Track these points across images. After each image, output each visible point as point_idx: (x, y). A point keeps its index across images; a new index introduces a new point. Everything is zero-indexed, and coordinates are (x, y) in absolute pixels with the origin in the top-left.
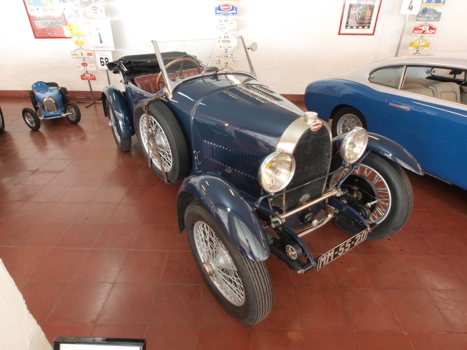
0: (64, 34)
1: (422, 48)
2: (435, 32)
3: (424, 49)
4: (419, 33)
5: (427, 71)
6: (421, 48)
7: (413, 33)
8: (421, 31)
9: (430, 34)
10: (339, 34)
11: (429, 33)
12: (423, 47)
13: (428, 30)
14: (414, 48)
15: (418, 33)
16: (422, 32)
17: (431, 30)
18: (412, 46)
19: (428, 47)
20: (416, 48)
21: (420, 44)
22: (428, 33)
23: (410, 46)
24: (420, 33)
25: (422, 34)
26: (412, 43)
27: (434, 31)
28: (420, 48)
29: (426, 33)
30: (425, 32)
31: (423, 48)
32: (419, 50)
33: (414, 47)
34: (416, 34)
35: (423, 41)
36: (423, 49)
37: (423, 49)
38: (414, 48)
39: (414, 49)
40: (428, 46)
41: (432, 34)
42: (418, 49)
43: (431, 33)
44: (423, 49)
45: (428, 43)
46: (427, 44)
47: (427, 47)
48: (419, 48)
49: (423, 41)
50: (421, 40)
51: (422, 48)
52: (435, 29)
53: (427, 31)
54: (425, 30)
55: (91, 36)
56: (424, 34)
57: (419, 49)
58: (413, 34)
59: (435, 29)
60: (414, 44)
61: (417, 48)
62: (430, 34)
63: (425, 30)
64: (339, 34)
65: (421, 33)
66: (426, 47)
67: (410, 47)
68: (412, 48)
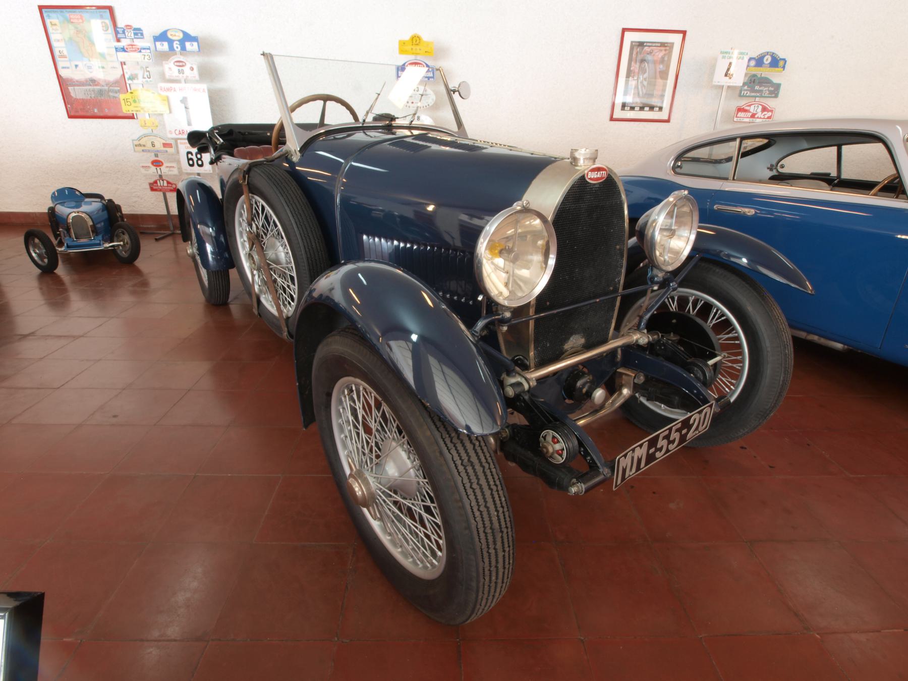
0: (122, 111)
2: (772, 115)
4: (745, 116)
5: (769, 166)
7: (736, 117)
8: (750, 114)
9: (764, 118)
10: (612, 119)
11: (763, 117)
13: (761, 113)
15: (743, 116)
16: (751, 116)
17: (765, 113)
22: (761, 118)
24: (748, 118)
25: (751, 119)
27: (770, 114)
29: (758, 118)
30: (756, 116)
34: (741, 119)
41: (767, 120)
43: (766, 117)
52: (772, 111)
53: (759, 114)
54: (755, 112)
55: (170, 112)
56: (754, 119)
58: (735, 119)
59: (772, 111)
62: (764, 120)
63: (756, 111)
64: (612, 119)
65: (749, 117)
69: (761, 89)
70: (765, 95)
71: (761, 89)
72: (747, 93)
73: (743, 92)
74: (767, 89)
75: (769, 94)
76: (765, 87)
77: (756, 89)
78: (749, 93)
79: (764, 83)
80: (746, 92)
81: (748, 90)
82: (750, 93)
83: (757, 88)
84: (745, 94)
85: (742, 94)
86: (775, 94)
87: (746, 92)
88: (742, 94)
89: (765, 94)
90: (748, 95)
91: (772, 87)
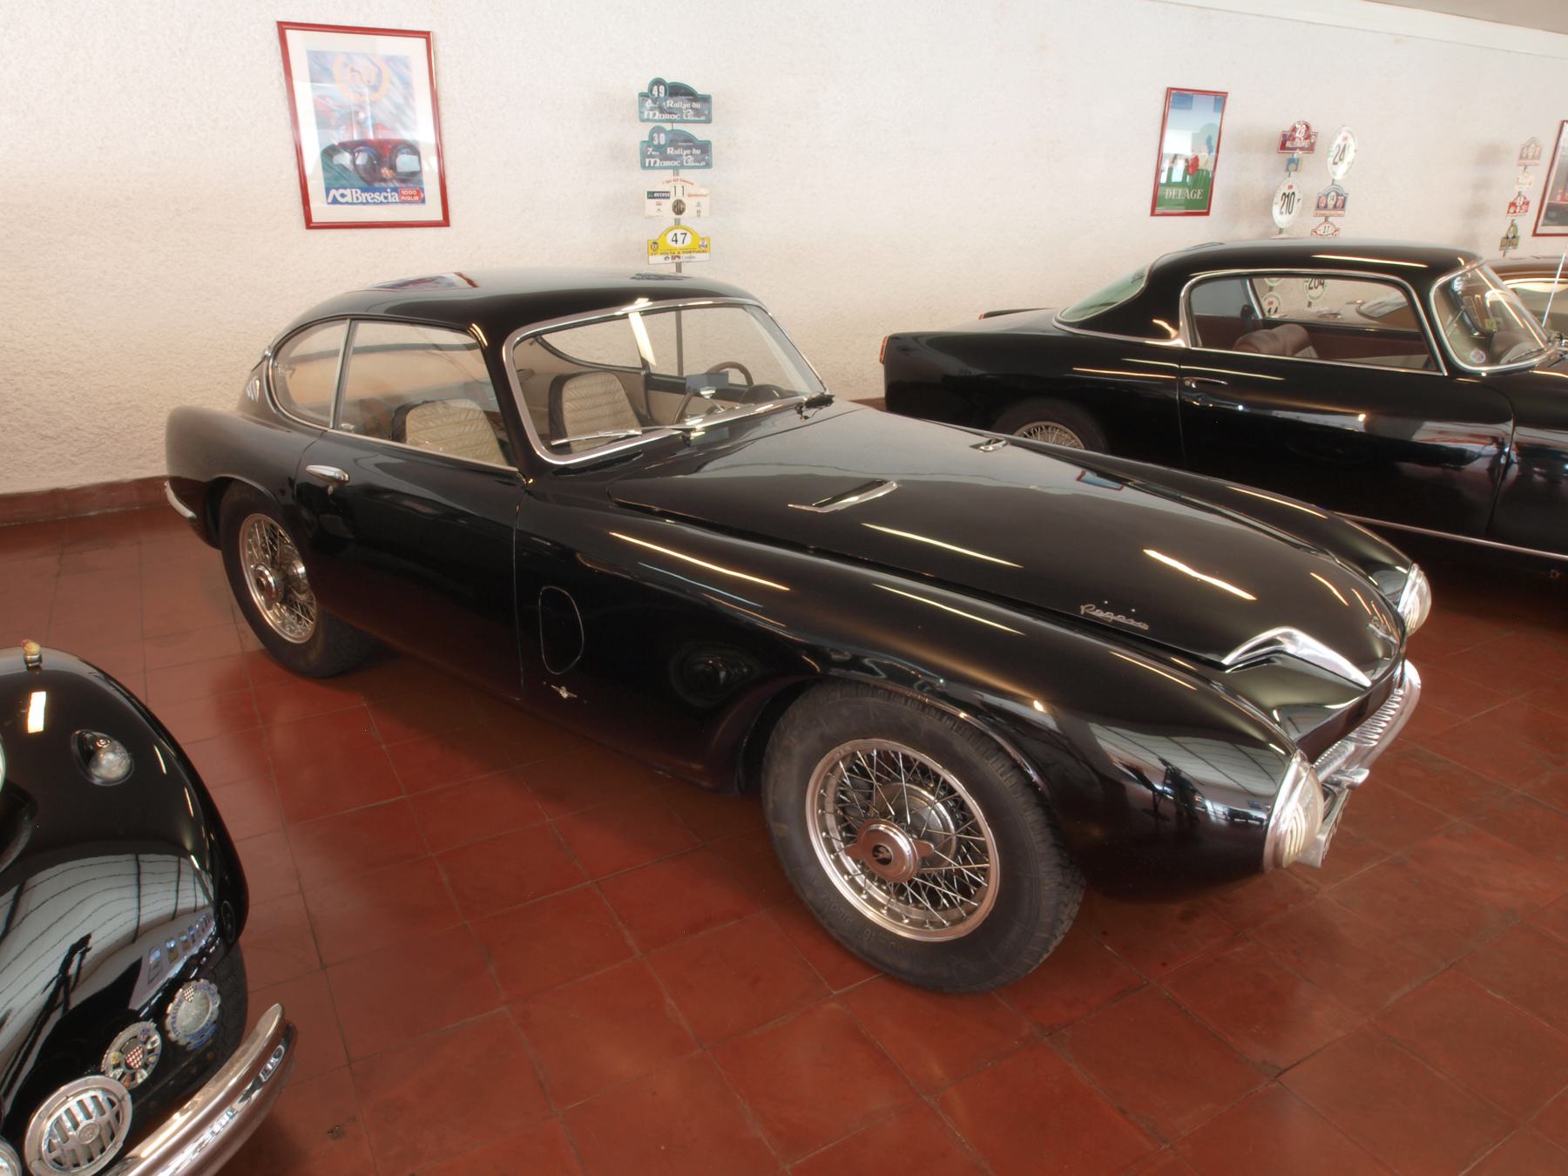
1: (690, 257)
3: (696, 260)
6: (685, 255)
12: (690, 252)
14: (666, 259)
18: (659, 251)
19: (706, 252)
21: (680, 244)
23: (651, 251)
26: (655, 243)
28: (683, 256)
31: (695, 255)
32: (683, 264)
35: (686, 234)
36: (694, 257)
37: (692, 260)
38: (666, 259)
39: (666, 262)
40: (704, 247)
42: (677, 260)
44: (694, 257)
45: (703, 239)
47: (703, 252)
48: (679, 257)
49: (686, 234)
50: (679, 232)
51: (690, 257)
60: (661, 247)
61: (673, 258)
66: (700, 252)
70: (689, 164)
71: (678, 152)
72: (655, 162)
73: (647, 160)
74: (689, 152)
75: (695, 162)
77: (668, 153)
78: (658, 161)
82: (661, 160)
83: (670, 151)
84: (652, 164)
85: (647, 165)
86: (704, 160)
87: (652, 160)
88: (647, 165)
89: (687, 162)
90: (657, 165)
91: (697, 149)
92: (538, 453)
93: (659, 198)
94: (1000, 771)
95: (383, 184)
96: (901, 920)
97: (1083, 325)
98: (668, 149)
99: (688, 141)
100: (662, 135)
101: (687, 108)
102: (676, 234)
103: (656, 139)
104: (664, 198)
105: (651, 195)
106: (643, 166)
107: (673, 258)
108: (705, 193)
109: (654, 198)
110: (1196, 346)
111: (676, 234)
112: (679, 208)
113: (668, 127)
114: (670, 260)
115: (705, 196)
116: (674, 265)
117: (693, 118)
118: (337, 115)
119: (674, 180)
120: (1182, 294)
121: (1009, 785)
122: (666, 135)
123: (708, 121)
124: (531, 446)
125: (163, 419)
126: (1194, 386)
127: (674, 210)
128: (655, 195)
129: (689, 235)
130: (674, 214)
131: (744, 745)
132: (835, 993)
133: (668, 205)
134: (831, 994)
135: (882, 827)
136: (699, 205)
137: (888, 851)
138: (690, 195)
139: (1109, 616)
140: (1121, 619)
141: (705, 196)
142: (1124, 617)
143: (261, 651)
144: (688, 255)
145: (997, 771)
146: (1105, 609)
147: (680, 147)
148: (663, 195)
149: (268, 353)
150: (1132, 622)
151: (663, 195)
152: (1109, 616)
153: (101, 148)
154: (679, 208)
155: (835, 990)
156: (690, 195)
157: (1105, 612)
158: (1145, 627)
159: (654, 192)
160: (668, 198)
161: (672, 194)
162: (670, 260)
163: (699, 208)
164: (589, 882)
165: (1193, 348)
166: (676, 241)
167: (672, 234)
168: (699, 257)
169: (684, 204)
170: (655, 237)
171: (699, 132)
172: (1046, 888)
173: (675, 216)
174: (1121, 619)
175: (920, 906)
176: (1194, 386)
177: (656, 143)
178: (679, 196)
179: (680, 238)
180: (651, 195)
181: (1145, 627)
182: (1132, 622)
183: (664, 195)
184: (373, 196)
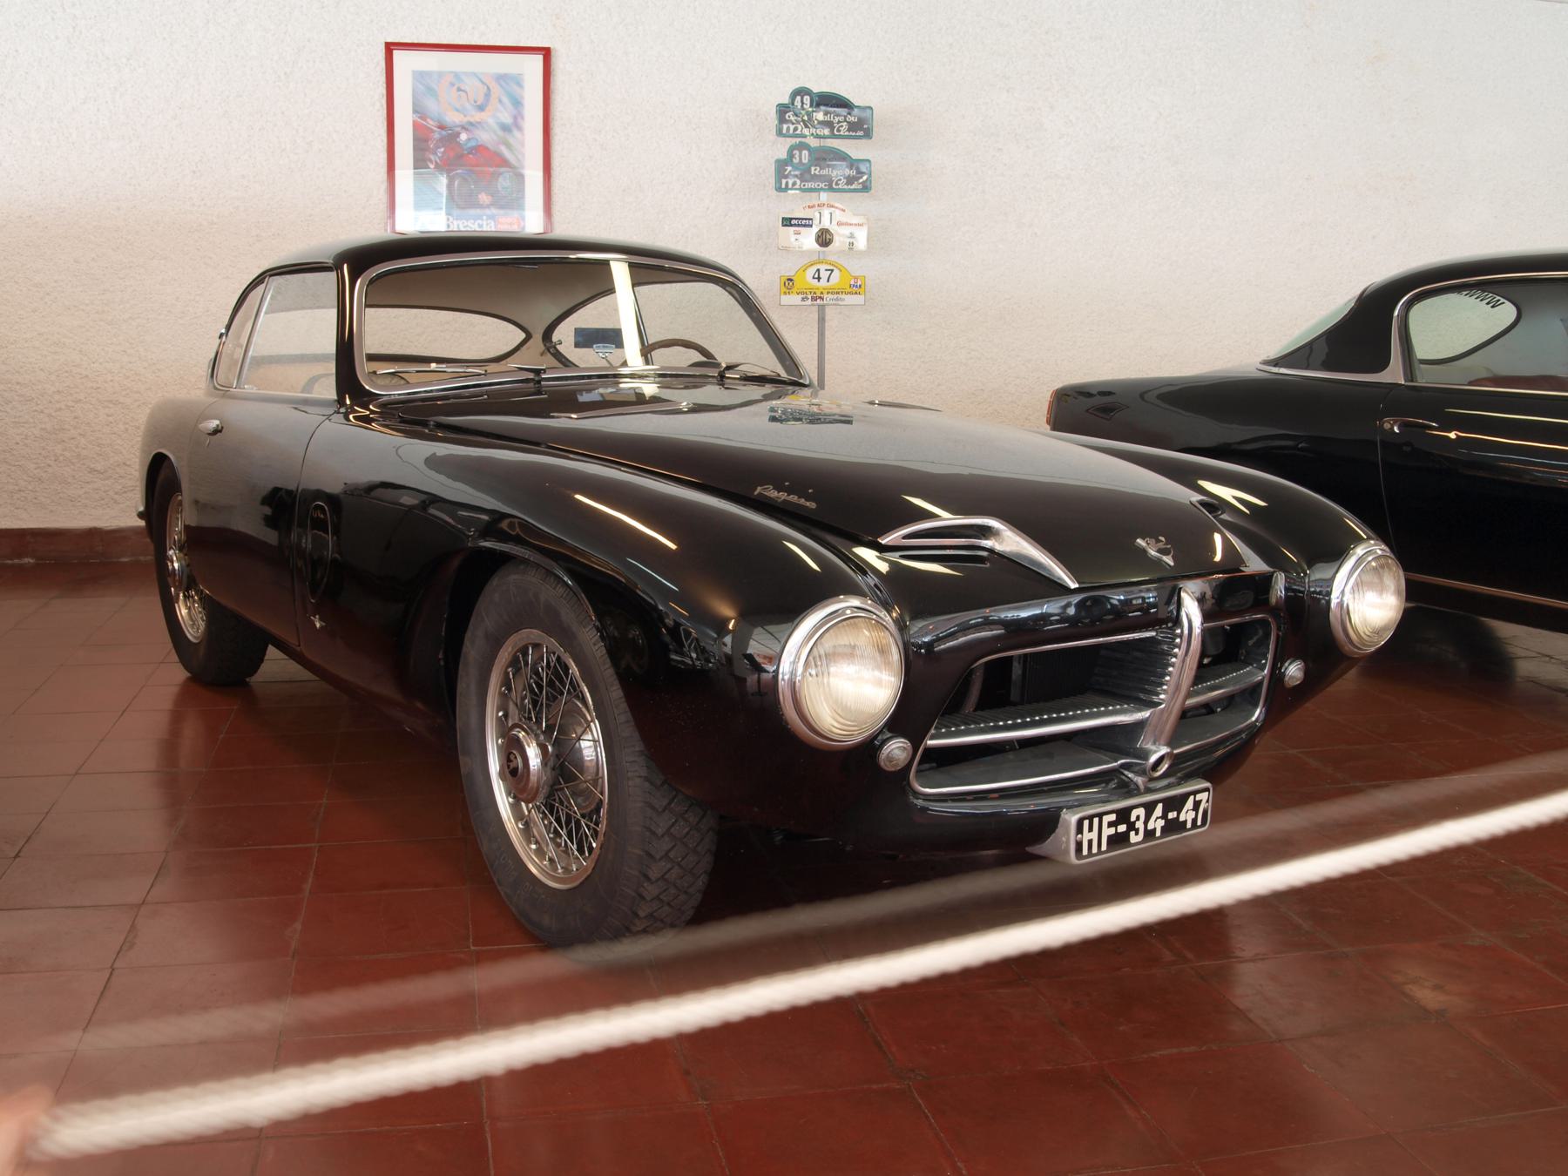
1: (837, 299)
6: (830, 296)
12: (838, 293)
14: (803, 299)
18: (795, 290)
20: (810, 297)
23: (784, 289)
26: (791, 280)
31: (843, 296)
32: (829, 312)
33: (800, 296)
35: (832, 271)
36: (843, 300)
37: (840, 303)
39: (804, 303)
40: (856, 288)
44: (843, 300)
45: (856, 278)
46: (852, 282)
47: (856, 293)
50: (822, 267)
51: (837, 299)
57: (825, 302)
60: (798, 284)
61: (814, 299)
66: (851, 293)
67: (785, 293)
68: (795, 299)
69: (825, 172)
71: (825, 172)
72: (794, 184)
73: (784, 181)
76: (833, 167)
78: (798, 182)
79: (830, 160)
80: (791, 182)
81: (796, 176)
82: (801, 181)
85: (783, 186)
89: (837, 184)
90: (797, 186)
92: (367, 387)
93: (799, 225)
94: (593, 641)
95: (478, 211)
96: (529, 842)
97: (1276, 362)
98: (813, 169)
99: (843, 157)
100: (805, 153)
101: (839, 122)
102: (818, 270)
103: (797, 156)
104: (805, 226)
105: (787, 222)
106: (779, 189)
107: (814, 299)
108: (861, 222)
109: (791, 225)
110: (1412, 381)
111: (818, 270)
112: (824, 239)
113: (814, 143)
114: (809, 302)
115: (860, 225)
116: (816, 308)
117: (847, 133)
118: (437, 136)
119: (818, 206)
120: (1396, 313)
121: (600, 655)
122: (810, 155)
123: (868, 134)
124: (359, 381)
125: (142, 417)
126: (1396, 429)
127: (817, 241)
128: (793, 222)
129: (836, 272)
130: (818, 247)
131: (442, 663)
132: (472, 948)
133: (808, 239)
134: (469, 947)
135: (522, 735)
136: (852, 236)
137: (516, 757)
138: (839, 224)
139: (783, 496)
140: (793, 498)
141: (860, 225)
142: (796, 497)
143: (189, 679)
144: (835, 296)
145: (591, 639)
146: (779, 489)
147: (829, 166)
148: (804, 222)
149: (223, 331)
150: (802, 501)
151: (804, 222)
152: (783, 496)
153: (194, 172)
154: (824, 239)
155: (474, 946)
156: (839, 224)
157: (779, 492)
158: (812, 505)
159: (791, 219)
160: (811, 226)
161: (816, 222)
162: (809, 302)
163: (851, 240)
164: (313, 845)
165: (1407, 384)
166: (819, 278)
167: (814, 269)
168: (850, 299)
169: (831, 234)
170: (790, 274)
171: (855, 149)
172: (630, 783)
173: (816, 247)
174: (793, 498)
175: (559, 840)
176: (1396, 429)
177: (796, 161)
178: (826, 224)
179: (825, 275)
180: (787, 222)
181: (812, 505)
182: (802, 501)
183: (805, 223)
184: (466, 224)
